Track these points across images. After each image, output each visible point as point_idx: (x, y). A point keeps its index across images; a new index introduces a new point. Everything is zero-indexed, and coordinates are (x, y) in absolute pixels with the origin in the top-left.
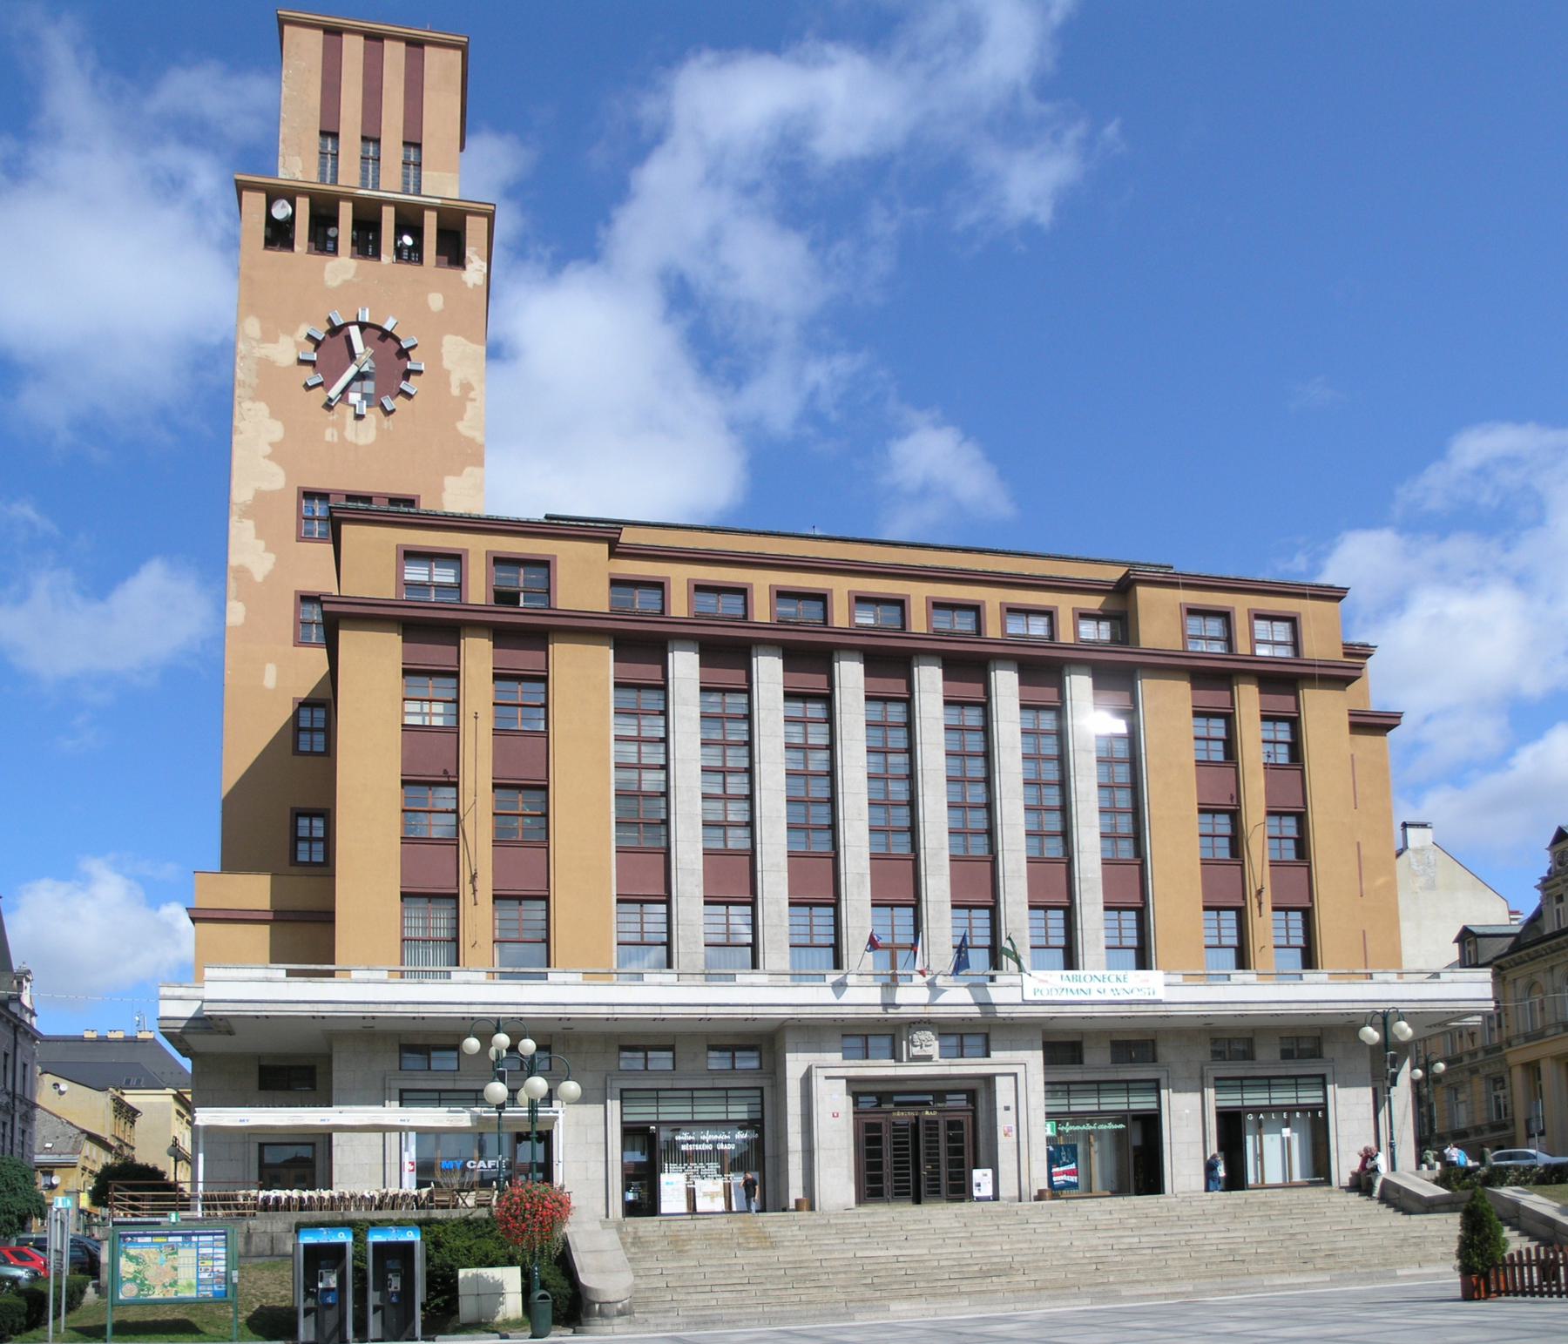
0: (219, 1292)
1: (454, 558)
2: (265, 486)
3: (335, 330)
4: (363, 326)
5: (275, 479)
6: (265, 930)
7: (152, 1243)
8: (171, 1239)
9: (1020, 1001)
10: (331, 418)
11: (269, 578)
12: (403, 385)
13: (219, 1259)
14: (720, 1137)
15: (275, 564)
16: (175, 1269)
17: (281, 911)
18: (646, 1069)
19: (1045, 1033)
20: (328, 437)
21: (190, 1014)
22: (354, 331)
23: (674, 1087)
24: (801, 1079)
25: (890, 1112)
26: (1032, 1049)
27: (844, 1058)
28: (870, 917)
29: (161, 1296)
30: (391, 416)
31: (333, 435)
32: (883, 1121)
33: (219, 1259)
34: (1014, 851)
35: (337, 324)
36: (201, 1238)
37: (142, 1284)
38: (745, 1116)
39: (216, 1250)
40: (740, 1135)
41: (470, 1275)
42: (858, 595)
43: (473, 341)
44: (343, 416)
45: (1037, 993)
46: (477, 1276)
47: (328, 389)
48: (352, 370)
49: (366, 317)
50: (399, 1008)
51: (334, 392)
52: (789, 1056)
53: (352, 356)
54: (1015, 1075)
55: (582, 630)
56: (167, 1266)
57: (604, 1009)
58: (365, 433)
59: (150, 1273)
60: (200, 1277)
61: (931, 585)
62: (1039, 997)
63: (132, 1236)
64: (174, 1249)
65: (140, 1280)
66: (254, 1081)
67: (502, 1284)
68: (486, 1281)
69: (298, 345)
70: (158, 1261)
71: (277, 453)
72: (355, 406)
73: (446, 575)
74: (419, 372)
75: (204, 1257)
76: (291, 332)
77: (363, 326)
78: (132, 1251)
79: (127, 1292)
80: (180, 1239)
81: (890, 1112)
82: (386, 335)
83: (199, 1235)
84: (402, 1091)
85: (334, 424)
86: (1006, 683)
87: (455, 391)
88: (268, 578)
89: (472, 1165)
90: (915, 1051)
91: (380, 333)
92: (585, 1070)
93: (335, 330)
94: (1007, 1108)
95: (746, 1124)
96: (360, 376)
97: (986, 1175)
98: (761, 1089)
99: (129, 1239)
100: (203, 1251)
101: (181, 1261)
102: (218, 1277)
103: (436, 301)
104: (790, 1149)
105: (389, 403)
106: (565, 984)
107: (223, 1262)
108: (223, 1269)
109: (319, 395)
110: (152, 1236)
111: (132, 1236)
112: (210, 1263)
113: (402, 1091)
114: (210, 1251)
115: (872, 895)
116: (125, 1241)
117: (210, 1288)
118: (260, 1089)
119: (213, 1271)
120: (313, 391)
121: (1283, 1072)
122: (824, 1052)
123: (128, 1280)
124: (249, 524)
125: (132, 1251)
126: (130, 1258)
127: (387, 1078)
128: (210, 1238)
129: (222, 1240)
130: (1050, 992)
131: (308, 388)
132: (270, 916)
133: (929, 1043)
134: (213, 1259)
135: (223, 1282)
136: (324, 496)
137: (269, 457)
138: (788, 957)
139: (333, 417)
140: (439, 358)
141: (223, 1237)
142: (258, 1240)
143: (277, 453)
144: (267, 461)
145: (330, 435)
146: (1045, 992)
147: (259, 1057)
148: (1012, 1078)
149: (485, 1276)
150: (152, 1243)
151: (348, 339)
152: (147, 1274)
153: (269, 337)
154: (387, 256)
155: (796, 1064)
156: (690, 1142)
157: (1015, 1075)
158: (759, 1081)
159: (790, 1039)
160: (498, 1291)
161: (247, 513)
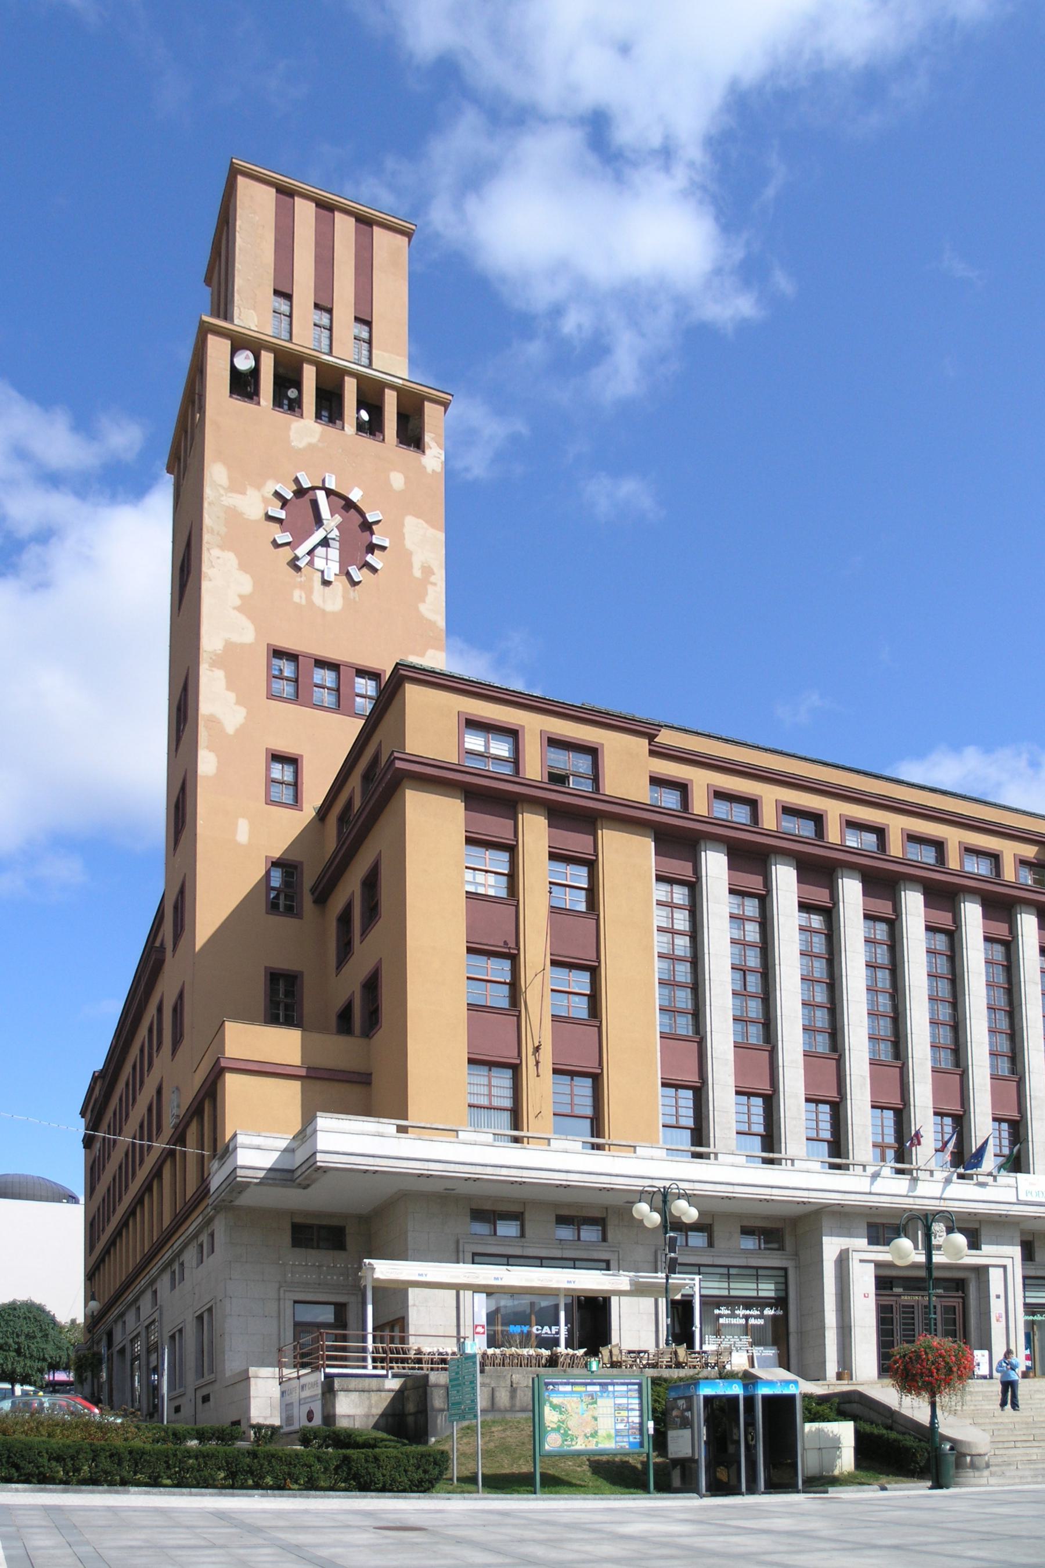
0: (634, 1442)
2: (236, 638)
3: (300, 492)
4: (329, 492)
5: (246, 633)
6: (296, 1086)
7: (572, 1392)
9: (1014, 1200)
10: (299, 579)
11: (240, 731)
12: (369, 558)
13: (633, 1410)
14: (752, 1312)
15: (245, 718)
17: (314, 1068)
18: (687, 1245)
19: (1023, 1233)
21: (269, 1166)
22: (321, 496)
23: (715, 1263)
24: (835, 1261)
25: (900, 1296)
26: (1013, 1245)
27: (870, 1243)
28: (870, 1117)
29: (583, 1447)
30: (357, 587)
31: (301, 597)
32: (894, 1303)
33: (633, 1410)
34: (981, 1066)
35: (305, 486)
36: (617, 1388)
38: (772, 1294)
39: (631, 1401)
40: (768, 1312)
41: (814, 1429)
42: (848, 819)
43: (433, 526)
44: (310, 580)
45: (1029, 1195)
46: (819, 1431)
47: (294, 549)
48: (319, 535)
49: (331, 484)
51: (302, 550)
52: (825, 1239)
53: (319, 521)
54: (1005, 1267)
56: (588, 1416)
60: (617, 1427)
61: (905, 817)
62: (1030, 1198)
63: (553, 1384)
65: (562, 1429)
66: (287, 1238)
67: (839, 1438)
68: (826, 1435)
69: (265, 500)
70: (580, 1411)
71: (247, 606)
74: (383, 548)
75: (618, 1408)
76: (259, 487)
77: (329, 492)
78: (556, 1400)
81: (900, 1296)
82: (349, 505)
83: (613, 1384)
84: (474, 1254)
85: (301, 586)
86: (972, 913)
87: (417, 573)
88: (238, 731)
89: (537, 1330)
91: (343, 502)
92: (637, 1243)
93: (300, 492)
95: (773, 1301)
96: (325, 543)
97: (983, 1356)
98: (785, 1269)
99: (551, 1387)
100: (619, 1401)
101: (600, 1411)
102: (633, 1428)
103: (397, 480)
104: (826, 1326)
105: (356, 574)
107: (637, 1413)
108: (637, 1420)
109: (286, 553)
110: (573, 1384)
111: (553, 1384)
112: (624, 1413)
113: (474, 1254)
114: (624, 1401)
115: (871, 1097)
116: (547, 1389)
117: (626, 1439)
118: (293, 1247)
119: (628, 1422)
120: (281, 549)
122: (854, 1237)
123: (553, 1429)
124: (220, 674)
125: (556, 1400)
127: (461, 1241)
128: (624, 1388)
129: (635, 1390)
130: (1038, 1193)
131: (276, 545)
132: (303, 1072)
134: (628, 1410)
135: (637, 1432)
136: (293, 657)
137: (238, 609)
138: (805, 1149)
139: (299, 578)
140: (402, 537)
141: (636, 1387)
142: (522, 1394)
143: (247, 606)
144: (236, 613)
146: (1034, 1194)
147: (292, 1213)
148: (1001, 1270)
149: (826, 1430)
150: (572, 1392)
151: (315, 504)
152: (570, 1424)
153: (236, 487)
154: (350, 428)
155: (831, 1246)
156: (727, 1316)
157: (1005, 1267)
158: (784, 1261)
159: (826, 1223)
160: (835, 1445)
161: (216, 663)
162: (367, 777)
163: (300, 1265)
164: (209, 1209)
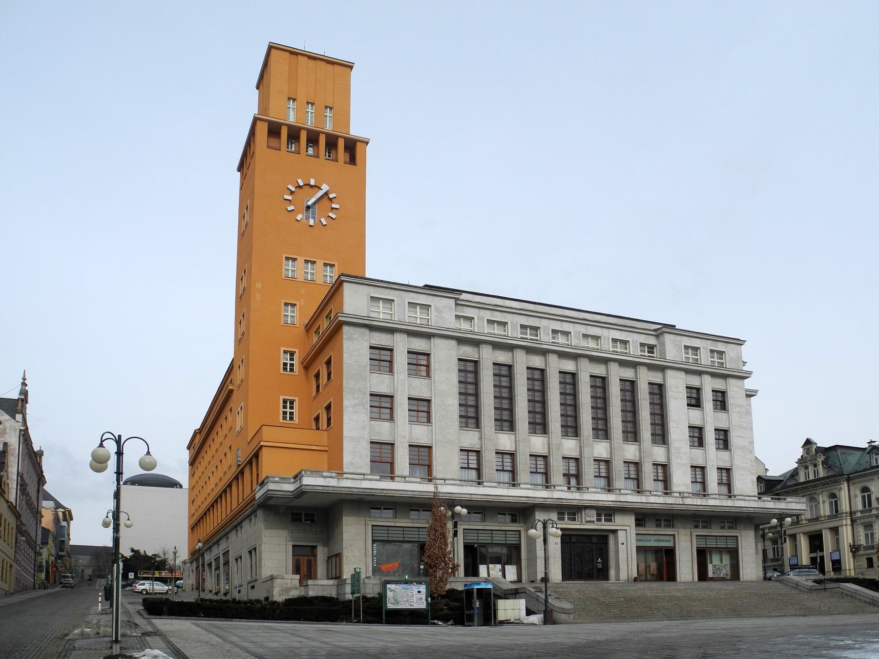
90: (588, 519)
94: (623, 544)
121: (721, 534)
133: (592, 515)
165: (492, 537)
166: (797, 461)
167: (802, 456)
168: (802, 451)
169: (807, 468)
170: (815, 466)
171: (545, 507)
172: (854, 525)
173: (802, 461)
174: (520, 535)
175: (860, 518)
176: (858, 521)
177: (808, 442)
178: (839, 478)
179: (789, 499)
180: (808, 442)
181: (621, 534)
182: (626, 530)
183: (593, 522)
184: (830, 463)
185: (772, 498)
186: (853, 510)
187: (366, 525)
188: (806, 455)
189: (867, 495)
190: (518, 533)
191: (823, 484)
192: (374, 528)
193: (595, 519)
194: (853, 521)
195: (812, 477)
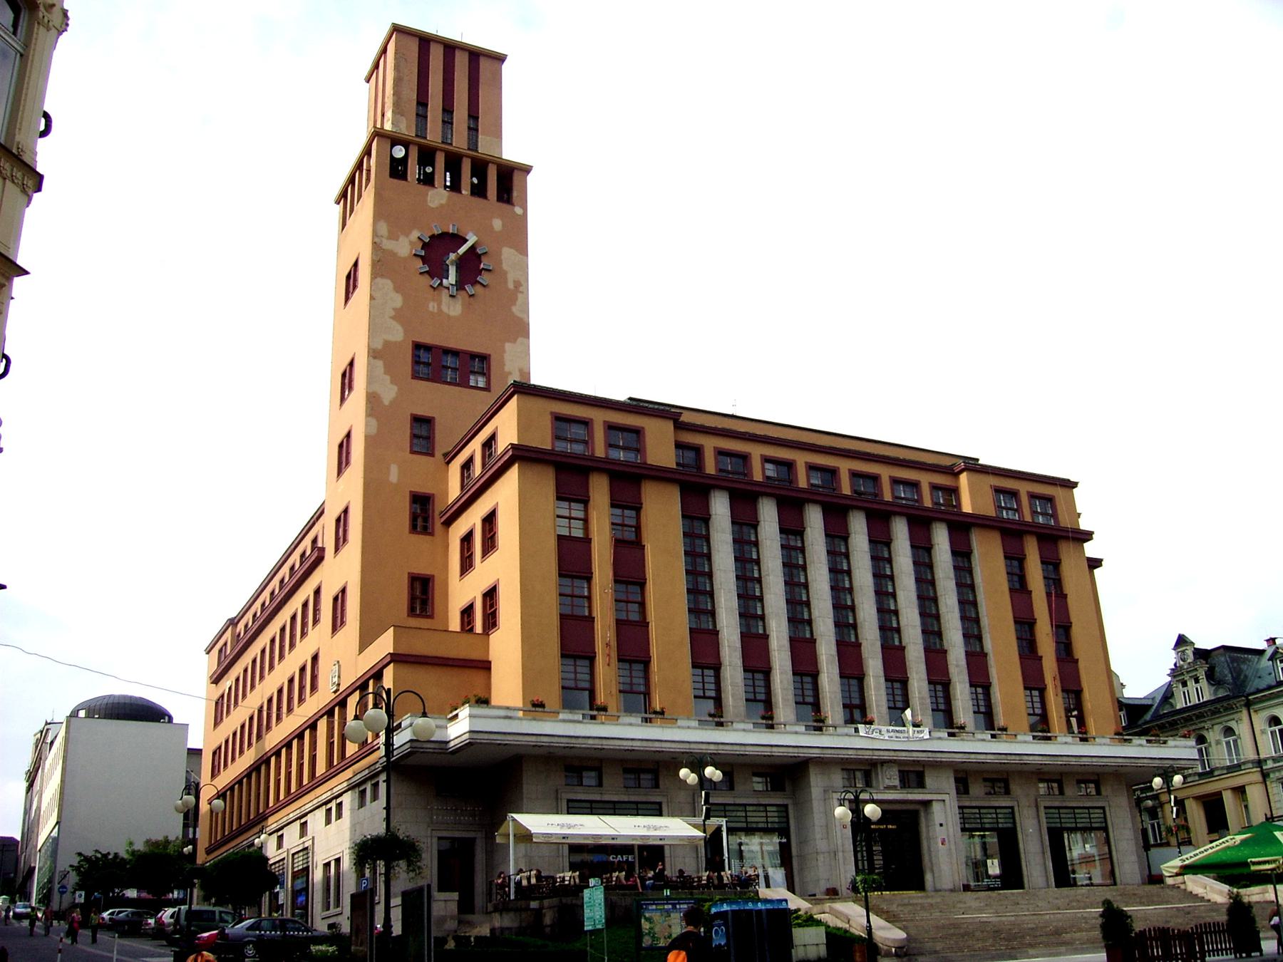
1: (586, 423)
2: (391, 338)
8: (666, 907)
16: (670, 926)
20: (431, 309)
37: (653, 937)
50: (590, 741)
55: (661, 475)
57: (712, 747)
58: (453, 308)
59: (656, 930)
64: (668, 912)
72: (448, 288)
73: (578, 431)
79: (647, 941)
80: (670, 906)
90: (887, 782)
106: (689, 728)
126: (647, 919)
137: (391, 318)
145: (432, 306)
162: (489, 444)
163: (442, 809)
164: (377, 765)
165: (746, 817)
166: (1169, 672)
167: (1175, 665)
168: (1175, 656)
169: (1184, 684)
170: (1197, 681)
171: (826, 762)
172: (1268, 783)
173: (1176, 672)
174: (787, 812)
175: (1274, 770)
176: (1272, 776)
177: (1182, 641)
178: (1235, 701)
179: (1171, 742)
180: (1182, 641)
181: (936, 807)
182: (944, 801)
183: (894, 788)
184: (1217, 675)
185: (1147, 740)
186: (1262, 756)
187: (557, 799)
188: (1182, 663)
189: (1279, 730)
190: (783, 809)
191: (1214, 713)
192: (571, 804)
193: (897, 782)
194: (1265, 775)
195: (1195, 701)
